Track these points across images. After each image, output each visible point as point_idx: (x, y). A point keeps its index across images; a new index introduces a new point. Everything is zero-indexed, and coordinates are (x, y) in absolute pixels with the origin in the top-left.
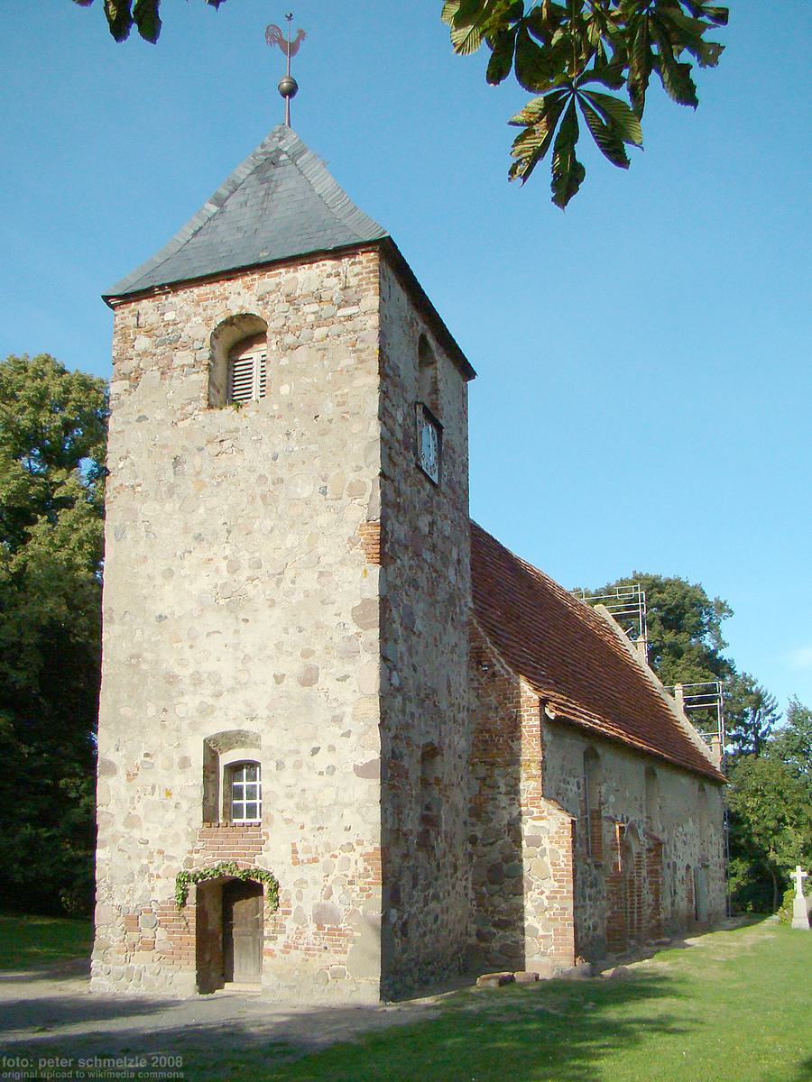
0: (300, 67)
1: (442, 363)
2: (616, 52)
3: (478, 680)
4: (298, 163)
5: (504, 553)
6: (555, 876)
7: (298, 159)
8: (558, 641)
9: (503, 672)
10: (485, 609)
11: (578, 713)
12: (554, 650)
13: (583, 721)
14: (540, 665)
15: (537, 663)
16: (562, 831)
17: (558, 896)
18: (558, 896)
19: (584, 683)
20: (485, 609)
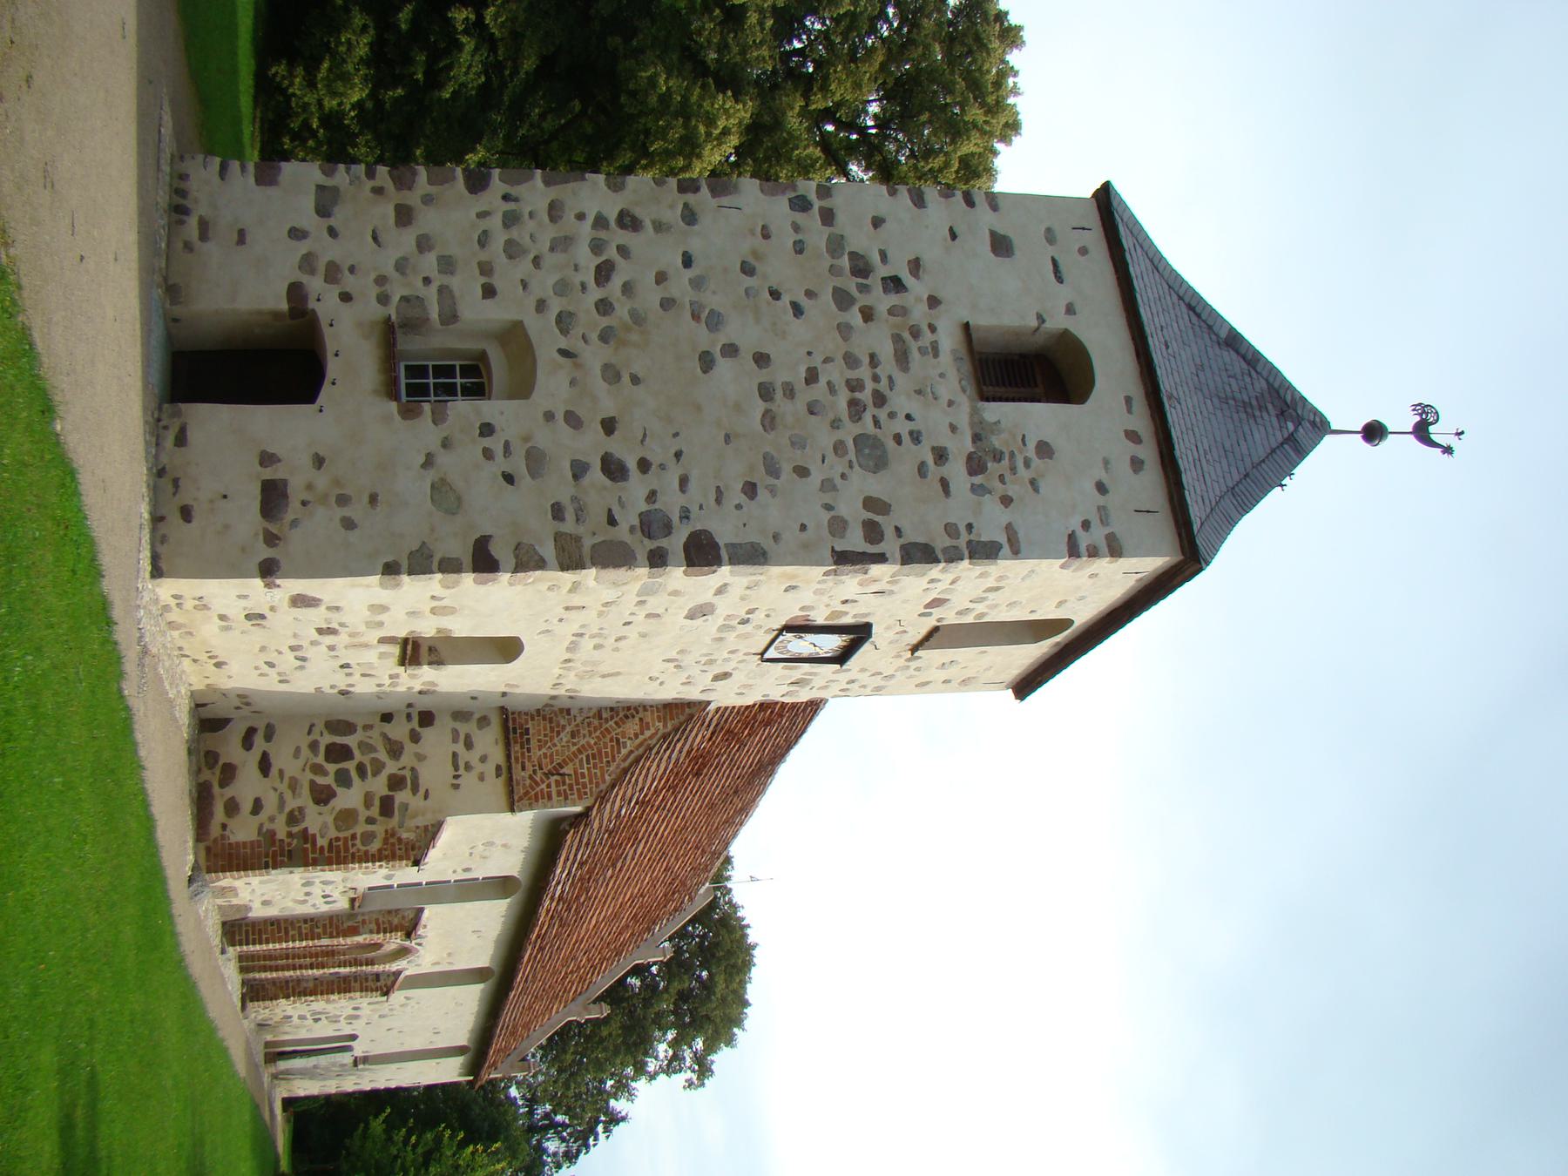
0: (1400, 447)
1: (1029, 654)
2: (588, 1139)
3: (612, 718)
4: (1285, 446)
5: (790, 744)
6: (338, 839)
7: (1291, 447)
8: (666, 833)
9: (624, 752)
10: (709, 726)
11: (569, 863)
12: (654, 826)
13: (558, 871)
14: (634, 807)
15: (637, 803)
16: (403, 846)
17: (309, 846)
18: (309, 846)
19: (610, 871)
20: (709, 726)
